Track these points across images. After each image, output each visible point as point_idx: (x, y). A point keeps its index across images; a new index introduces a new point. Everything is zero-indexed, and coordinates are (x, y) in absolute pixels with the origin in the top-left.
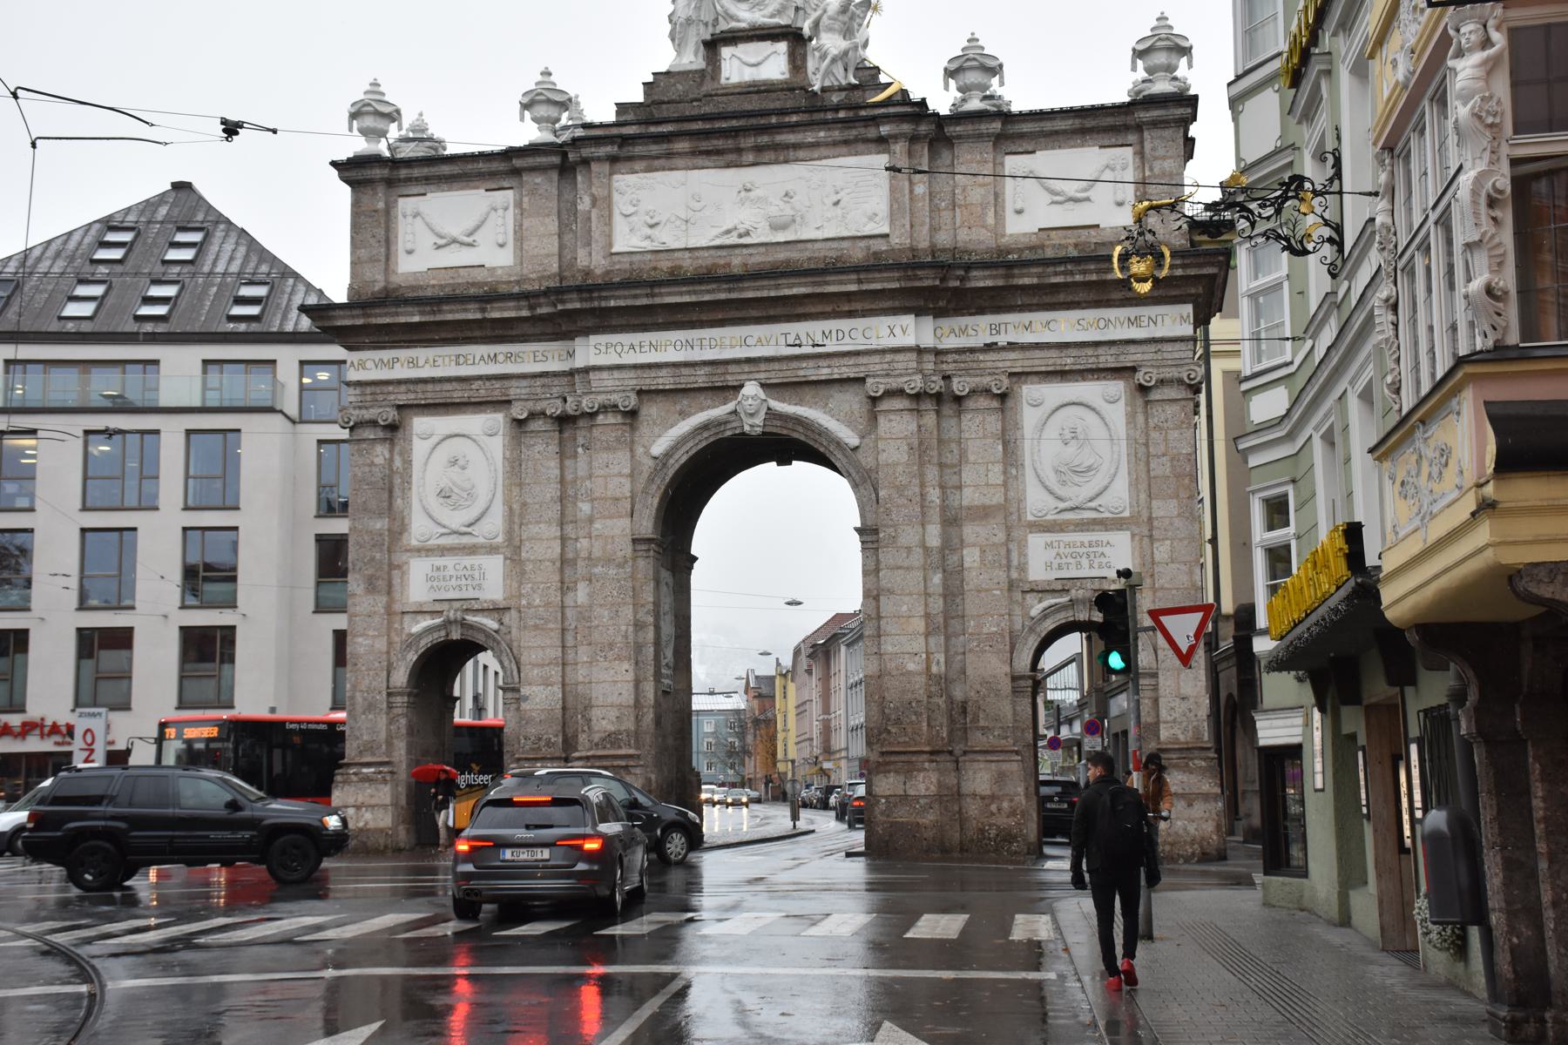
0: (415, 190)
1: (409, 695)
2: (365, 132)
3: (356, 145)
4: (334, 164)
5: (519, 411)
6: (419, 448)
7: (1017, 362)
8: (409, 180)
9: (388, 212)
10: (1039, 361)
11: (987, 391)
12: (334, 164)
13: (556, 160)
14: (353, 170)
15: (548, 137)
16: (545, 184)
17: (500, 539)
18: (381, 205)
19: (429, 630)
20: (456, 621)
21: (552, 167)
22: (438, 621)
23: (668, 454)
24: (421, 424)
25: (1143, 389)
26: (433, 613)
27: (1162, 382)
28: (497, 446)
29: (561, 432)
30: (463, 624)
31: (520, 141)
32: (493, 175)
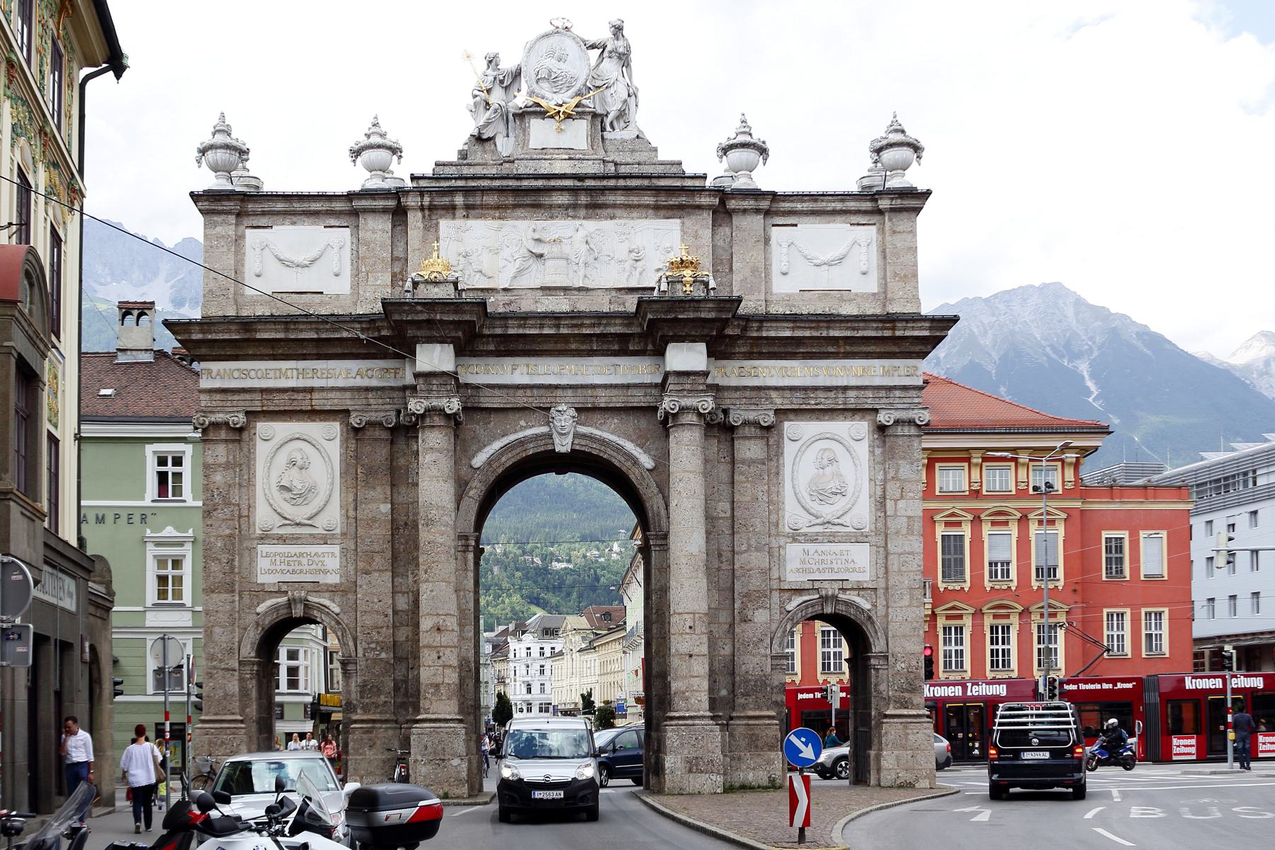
0: (263, 221)
1: (259, 664)
2: (215, 168)
3: (209, 181)
4: (192, 195)
5: (354, 421)
6: (262, 450)
7: (779, 401)
8: (255, 214)
9: (239, 239)
10: (795, 402)
11: (756, 424)
12: (192, 195)
13: (391, 203)
14: (208, 201)
15: (376, 183)
16: (378, 228)
17: (338, 531)
18: (232, 233)
19: (275, 608)
20: (301, 601)
21: (385, 211)
22: (283, 600)
23: (489, 462)
24: (262, 427)
25: (882, 429)
26: (280, 592)
27: (897, 422)
28: (334, 450)
29: (392, 442)
30: (307, 605)
31: (357, 188)
32: (331, 213)
